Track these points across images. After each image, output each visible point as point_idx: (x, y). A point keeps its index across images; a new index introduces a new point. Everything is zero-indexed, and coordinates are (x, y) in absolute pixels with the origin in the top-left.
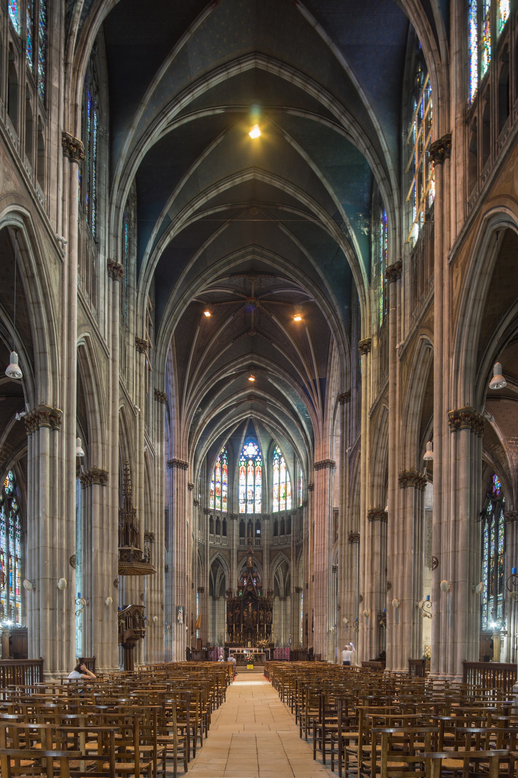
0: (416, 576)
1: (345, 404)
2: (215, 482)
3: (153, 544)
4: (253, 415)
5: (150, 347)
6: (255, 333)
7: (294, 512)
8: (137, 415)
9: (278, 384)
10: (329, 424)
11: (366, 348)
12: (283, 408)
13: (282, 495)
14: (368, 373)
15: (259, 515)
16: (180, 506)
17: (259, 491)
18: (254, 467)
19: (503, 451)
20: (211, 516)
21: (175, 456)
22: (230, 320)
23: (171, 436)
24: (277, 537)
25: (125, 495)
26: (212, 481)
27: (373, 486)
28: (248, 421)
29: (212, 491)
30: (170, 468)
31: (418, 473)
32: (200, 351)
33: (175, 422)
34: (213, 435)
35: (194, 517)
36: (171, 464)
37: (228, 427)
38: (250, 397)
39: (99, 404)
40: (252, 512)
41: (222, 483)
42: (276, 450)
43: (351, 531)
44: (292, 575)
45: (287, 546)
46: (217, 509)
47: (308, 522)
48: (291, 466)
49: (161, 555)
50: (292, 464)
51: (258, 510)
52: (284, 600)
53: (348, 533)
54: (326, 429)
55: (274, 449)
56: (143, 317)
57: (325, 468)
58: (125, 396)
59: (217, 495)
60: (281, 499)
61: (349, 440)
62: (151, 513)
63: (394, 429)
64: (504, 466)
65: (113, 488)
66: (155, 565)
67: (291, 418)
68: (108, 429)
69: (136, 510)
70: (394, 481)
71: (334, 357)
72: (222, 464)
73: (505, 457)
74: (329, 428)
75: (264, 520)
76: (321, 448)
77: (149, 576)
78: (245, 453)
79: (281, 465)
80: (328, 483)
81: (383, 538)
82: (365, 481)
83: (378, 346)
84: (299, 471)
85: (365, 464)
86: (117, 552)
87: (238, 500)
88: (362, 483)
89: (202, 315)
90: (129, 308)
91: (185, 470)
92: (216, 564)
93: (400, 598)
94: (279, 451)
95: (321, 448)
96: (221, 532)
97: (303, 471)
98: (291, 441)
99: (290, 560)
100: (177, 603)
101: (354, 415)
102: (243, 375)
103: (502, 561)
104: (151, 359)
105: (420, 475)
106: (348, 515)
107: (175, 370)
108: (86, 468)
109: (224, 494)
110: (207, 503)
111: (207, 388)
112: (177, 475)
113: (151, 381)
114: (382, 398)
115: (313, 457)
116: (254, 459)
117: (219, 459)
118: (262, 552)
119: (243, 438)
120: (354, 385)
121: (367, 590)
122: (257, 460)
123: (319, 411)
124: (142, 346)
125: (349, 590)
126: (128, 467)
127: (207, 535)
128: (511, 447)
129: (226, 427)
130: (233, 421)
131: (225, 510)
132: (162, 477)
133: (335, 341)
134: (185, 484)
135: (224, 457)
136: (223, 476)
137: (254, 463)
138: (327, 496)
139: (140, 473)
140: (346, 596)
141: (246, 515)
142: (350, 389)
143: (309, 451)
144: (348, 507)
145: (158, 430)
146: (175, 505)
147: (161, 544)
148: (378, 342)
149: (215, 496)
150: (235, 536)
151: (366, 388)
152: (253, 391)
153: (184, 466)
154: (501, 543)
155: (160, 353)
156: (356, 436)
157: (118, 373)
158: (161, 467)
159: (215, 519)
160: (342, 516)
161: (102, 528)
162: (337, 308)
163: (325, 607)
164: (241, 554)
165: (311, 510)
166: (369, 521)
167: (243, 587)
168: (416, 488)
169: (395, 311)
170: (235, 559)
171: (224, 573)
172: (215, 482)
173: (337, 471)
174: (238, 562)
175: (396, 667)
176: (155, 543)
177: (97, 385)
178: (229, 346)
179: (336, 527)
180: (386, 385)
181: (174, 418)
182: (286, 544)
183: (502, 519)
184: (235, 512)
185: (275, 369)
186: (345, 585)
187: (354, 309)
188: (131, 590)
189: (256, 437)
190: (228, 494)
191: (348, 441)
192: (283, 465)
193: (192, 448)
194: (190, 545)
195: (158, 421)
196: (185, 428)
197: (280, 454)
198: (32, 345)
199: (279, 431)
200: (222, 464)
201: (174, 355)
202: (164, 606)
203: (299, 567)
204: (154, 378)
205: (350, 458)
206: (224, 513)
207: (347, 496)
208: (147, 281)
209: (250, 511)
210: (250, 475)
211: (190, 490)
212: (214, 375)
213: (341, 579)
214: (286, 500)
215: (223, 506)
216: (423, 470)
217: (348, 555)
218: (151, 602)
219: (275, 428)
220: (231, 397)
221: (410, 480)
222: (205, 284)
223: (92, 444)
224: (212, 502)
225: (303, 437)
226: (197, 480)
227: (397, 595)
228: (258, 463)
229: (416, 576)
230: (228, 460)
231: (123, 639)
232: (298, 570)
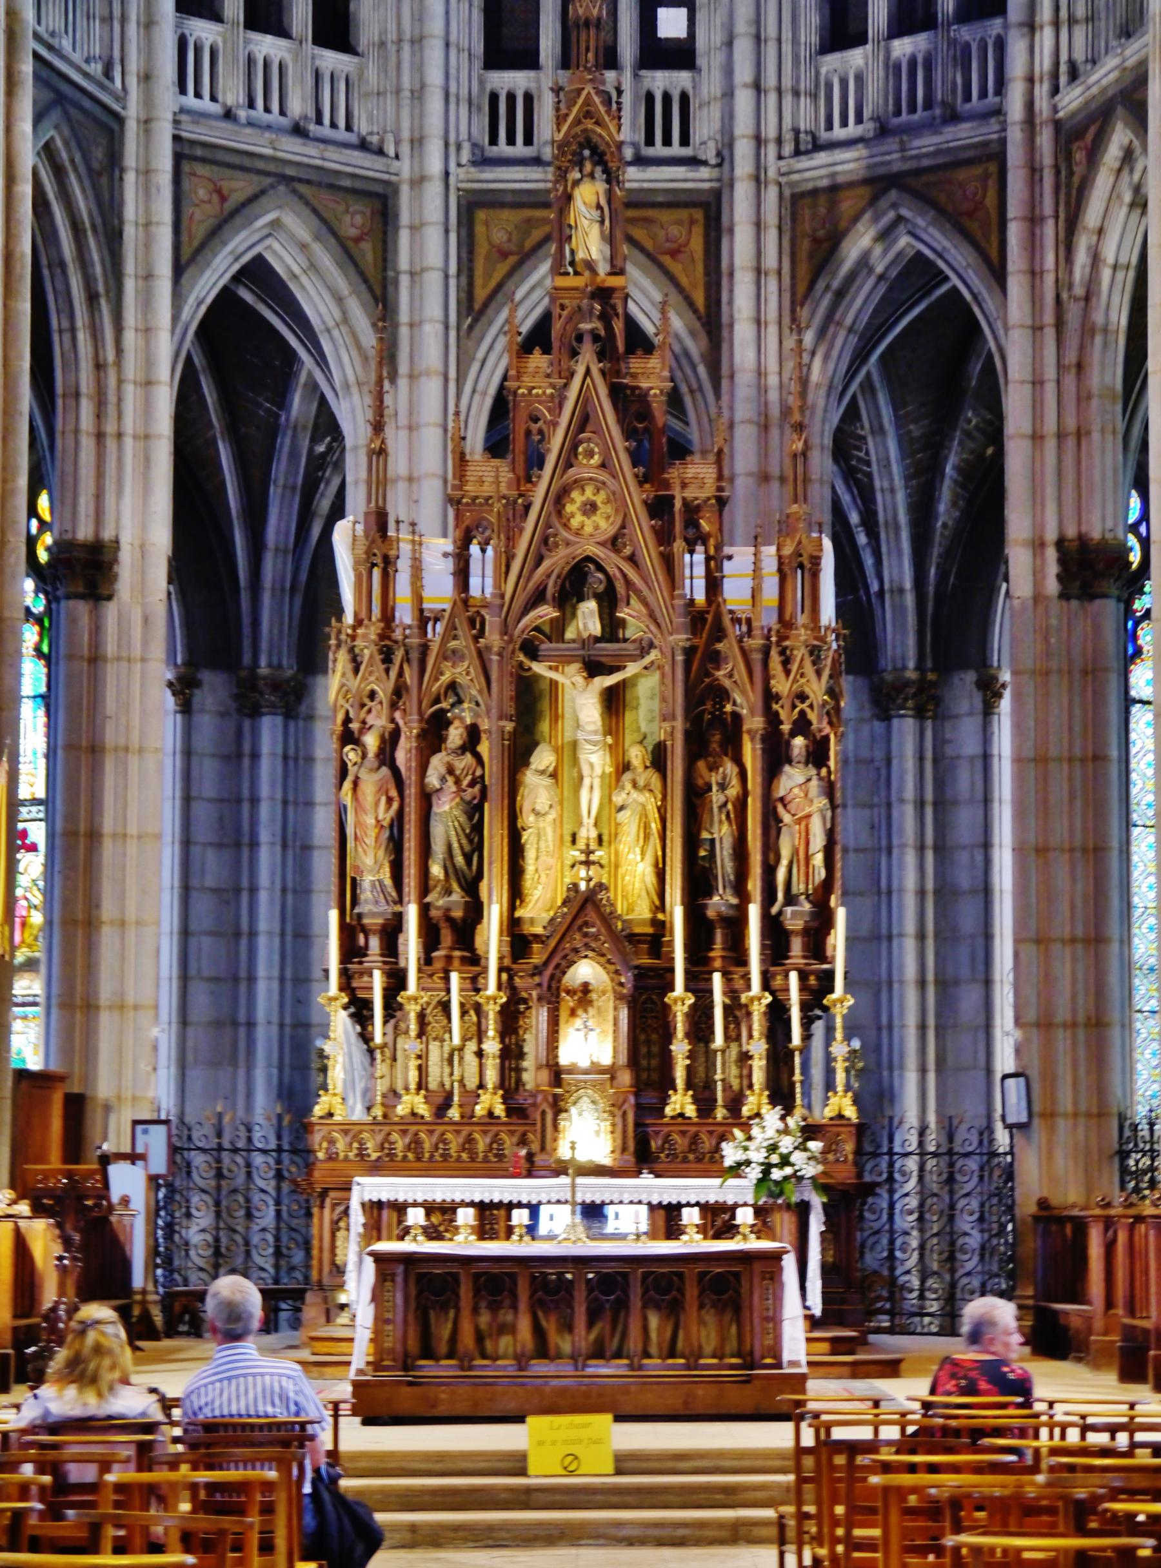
24: (856, 57)
99: (998, 275)
150: (434, 54)
182: (953, 117)
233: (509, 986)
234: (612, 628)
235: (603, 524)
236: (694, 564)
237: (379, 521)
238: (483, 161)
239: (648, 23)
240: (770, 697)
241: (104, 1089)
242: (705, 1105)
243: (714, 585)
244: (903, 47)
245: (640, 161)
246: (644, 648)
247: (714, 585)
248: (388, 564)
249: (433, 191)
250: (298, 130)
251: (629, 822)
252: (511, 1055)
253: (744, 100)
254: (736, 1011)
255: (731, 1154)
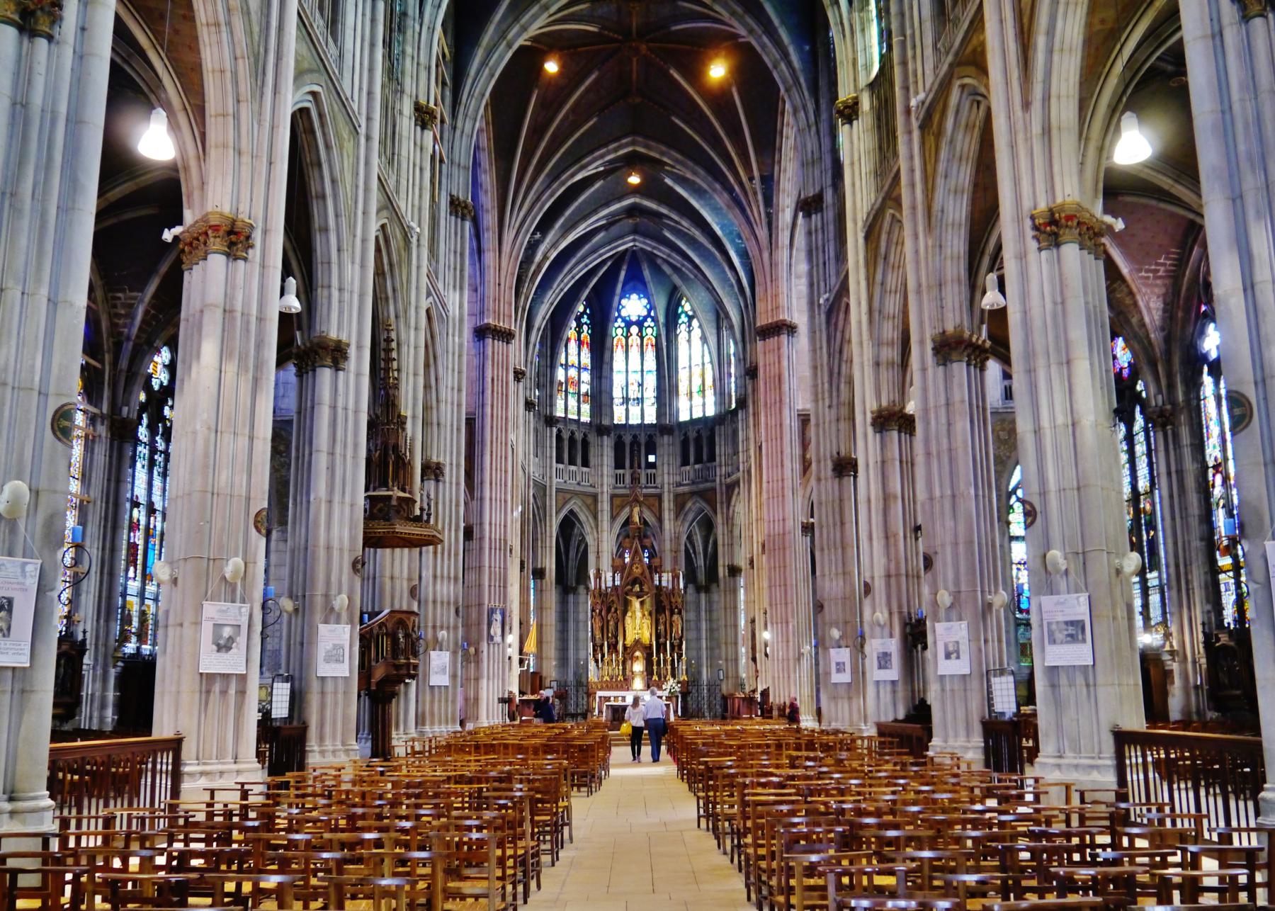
0: (984, 542)
1: (814, 216)
2: (566, 366)
3: (441, 484)
4: (637, 244)
5: (442, 121)
6: (638, 100)
7: (720, 419)
8: (414, 240)
9: (683, 188)
10: (783, 255)
11: (850, 113)
12: (693, 229)
13: (695, 388)
14: (856, 158)
15: (651, 425)
16: (498, 411)
17: (651, 381)
18: (642, 338)
19: (1131, 293)
20: (559, 431)
21: (488, 317)
22: (593, 77)
23: (482, 282)
24: (688, 468)
25: (385, 388)
26: (562, 365)
27: (877, 364)
28: (629, 254)
29: (561, 384)
30: (479, 341)
31: (971, 336)
32: (537, 132)
33: (490, 258)
34: (562, 281)
35: (526, 432)
36: (481, 333)
37: (591, 266)
38: (632, 211)
39: (337, 216)
40: (639, 422)
41: (580, 368)
42: (683, 307)
43: (838, 453)
44: (720, 542)
45: (708, 485)
46: (570, 416)
47: (747, 439)
48: (711, 334)
49: (457, 505)
50: (714, 331)
51: (651, 418)
52: (706, 592)
53: (831, 457)
54: (777, 265)
55: (679, 304)
56: (429, 68)
57: (779, 335)
58: (389, 204)
59: (571, 390)
60: (695, 395)
61: (825, 281)
62: (438, 424)
63: (917, 252)
64: (1134, 320)
65: (358, 375)
66: (443, 528)
67: (710, 247)
68: (353, 263)
69: (406, 417)
70: (921, 353)
71: (787, 138)
72: (579, 333)
73: (1136, 304)
74: (782, 263)
75: (662, 435)
76: (769, 299)
77: (431, 548)
78: (624, 313)
79: (692, 333)
80: (785, 363)
81: (908, 465)
82: (862, 355)
83: (872, 107)
84: (728, 344)
85: (860, 322)
86: (361, 501)
87: (612, 399)
88: (856, 360)
89: (540, 69)
90: (403, 52)
91: (508, 343)
92: (568, 525)
93: (951, 588)
94: (687, 307)
95: (769, 299)
96: (579, 461)
97: (736, 343)
98: (711, 290)
100: (490, 602)
101: (831, 235)
102: (618, 173)
103: (1148, 507)
104: (445, 142)
105: (974, 339)
106: (830, 422)
107: (491, 164)
108: (306, 337)
109: (585, 388)
110: (552, 405)
111: (551, 196)
112: (493, 353)
113: (444, 181)
114: (889, 198)
115: (754, 318)
116: (640, 324)
117: (574, 324)
118: (659, 497)
119: (619, 286)
120: (829, 181)
121: (879, 572)
122: (646, 324)
123: (762, 233)
124: (427, 117)
125: (840, 570)
126: (393, 335)
127: (551, 467)
128: (1146, 285)
129: (586, 266)
130: (601, 255)
131: (585, 418)
132: (460, 356)
133: (787, 106)
134: (507, 369)
135: (585, 320)
136: (582, 354)
137: (640, 331)
138: (786, 387)
139: (416, 348)
140: (834, 583)
141: (626, 427)
142: (822, 189)
143: (746, 306)
144: (830, 407)
145: (455, 269)
146: (488, 410)
147: (458, 484)
148: (872, 102)
149: (566, 391)
150: (605, 468)
151: (853, 185)
152: (637, 200)
153: (507, 336)
154: (1143, 470)
155: (462, 132)
156: (838, 273)
157: (375, 161)
158: (460, 336)
159: (566, 435)
160: (817, 425)
161: (332, 454)
162: (791, 50)
163: (789, 606)
164: (617, 501)
165: (754, 414)
166: (875, 432)
167: (624, 566)
168: (968, 365)
169: (903, 44)
170: (605, 513)
171: (584, 538)
172: (566, 366)
173: (802, 340)
174: (613, 518)
175: (956, 736)
176: (444, 482)
177: (333, 181)
178: (591, 123)
179: (805, 445)
180: (892, 175)
181: (489, 250)
182: (707, 481)
183: (1139, 422)
184: (606, 422)
185: (677, 161)
186: (830, 560)
187: (821, 51)
188: (392, 578)
189: (644, 284)
190: (592, 388)
191: (822, 284)
192: (697, 333)
193: (522, 303)
194: (517, 486)
195: (455, 252)
196: (510, 268)
197: (690, 313)
198: (204, 101)
199: (687, 272)
200: (579, 333)
201: (489, 140)
202: (461, 609)
203: (733, 525)
204: (450, 176)
205: (829, 313)
206: (584, 424)
207: (826, 386)
208: (439, 6)
209: (635, 420)
210: (634, 353)
211: (519, 381)
212: (563, 172)
213: (822, 549)
214: (704, 397)
215: (582, 410)
216: (980, 329)
217: (833, 501)
218: (434, 602)
219: (679, 265)
220: (595, 211)
221: (955, 349)
222: (546, 15)
223: (319, 290)
224: (560, 403)
225: (734, 282)
226: (531, 363)
227: (945, 581)
228: (649, 331)
229: (984, 542)
230: (592, 326)
231: (369, 683)
232: (732, 532)
233: (623, 656)
234: (641, 590)
235: (639, 571)
236: (656, 577)
237: (598, 570)
238: (615, 488)
239: (647, 459)
240: (671, 602)
241: (544, 674)
242: (660, 677)
243: (660, 581)
244: (697, 466)
245: (646, 487)
246: (647, 593)
247: (660, 581)
248: (600, 578)
249: (605, 495)
250: (579, 484)
251: (645, 626)
252: (624, 669)
253: (666, 476)
254: (665, 661)
255: (664, 687)
